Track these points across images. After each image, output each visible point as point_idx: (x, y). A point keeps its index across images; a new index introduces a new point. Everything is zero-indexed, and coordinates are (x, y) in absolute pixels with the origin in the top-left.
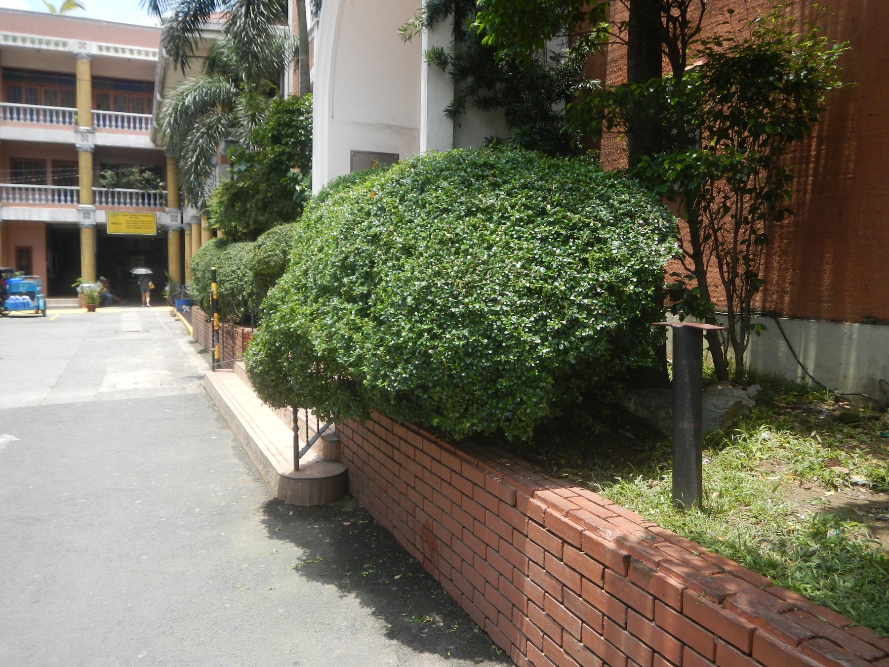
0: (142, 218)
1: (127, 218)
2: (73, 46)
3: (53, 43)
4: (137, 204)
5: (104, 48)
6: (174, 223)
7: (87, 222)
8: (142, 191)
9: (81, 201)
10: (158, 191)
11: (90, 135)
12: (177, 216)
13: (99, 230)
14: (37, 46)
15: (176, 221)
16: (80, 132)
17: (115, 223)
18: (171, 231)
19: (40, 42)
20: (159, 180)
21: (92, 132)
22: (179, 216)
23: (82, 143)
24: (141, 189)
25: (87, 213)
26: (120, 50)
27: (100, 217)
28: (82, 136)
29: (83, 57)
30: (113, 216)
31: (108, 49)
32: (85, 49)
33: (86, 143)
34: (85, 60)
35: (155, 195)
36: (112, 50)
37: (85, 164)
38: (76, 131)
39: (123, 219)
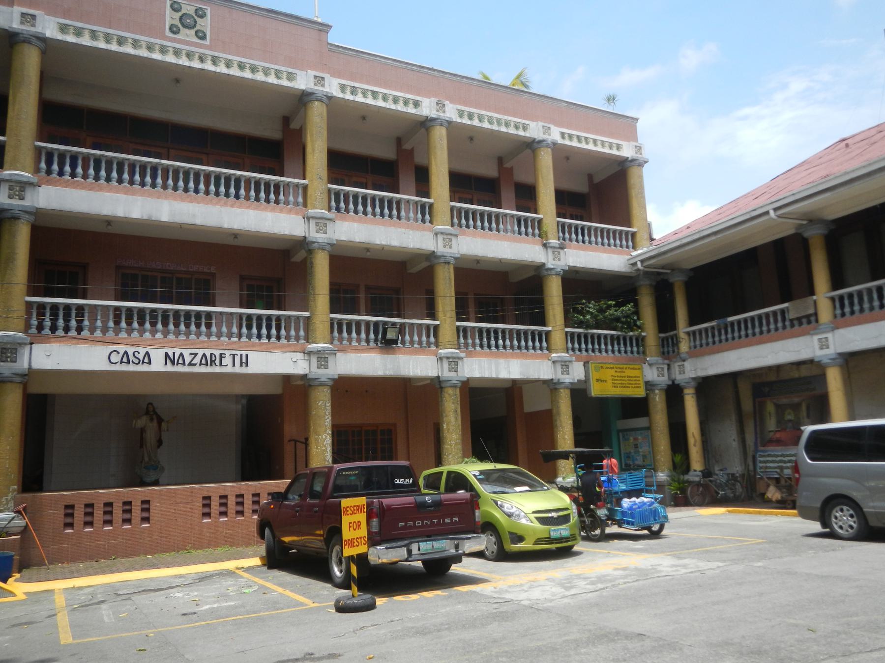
0: (629, 372)
1: (612, 372)
2: (534, 130)
3: (512, 124)
4: (613, 352)
5: (566, 136)
6: (661, 379)
7: (567, 379)
8: (619, 333)
9: (553, 347)
10: (636, 333)
11: (562, 252)
12: (663, 369)
13: (579, 393)
14: (495, 127)
15: (663, 376)
16: (551, 247)
17: (598, 380)
18: (657, 392)
19: (499, 122)
20: (635, 318)
21: (562, 247)
22: (666, 367)
23: (554, 262)
24: (621, 331)
25: (565, 366)
26: (583, 139)
27: (577, 373)
28: (553, 253)
29: (547, 146)
30: (597, 369)
31: (571, 137)
32: (549, 135)
33: (557, 262)
34: (549, 150)
35: (631, 339)
36: (575, 139)
37: (554, 292)
38: (545, 246)
39: (608, 374)
